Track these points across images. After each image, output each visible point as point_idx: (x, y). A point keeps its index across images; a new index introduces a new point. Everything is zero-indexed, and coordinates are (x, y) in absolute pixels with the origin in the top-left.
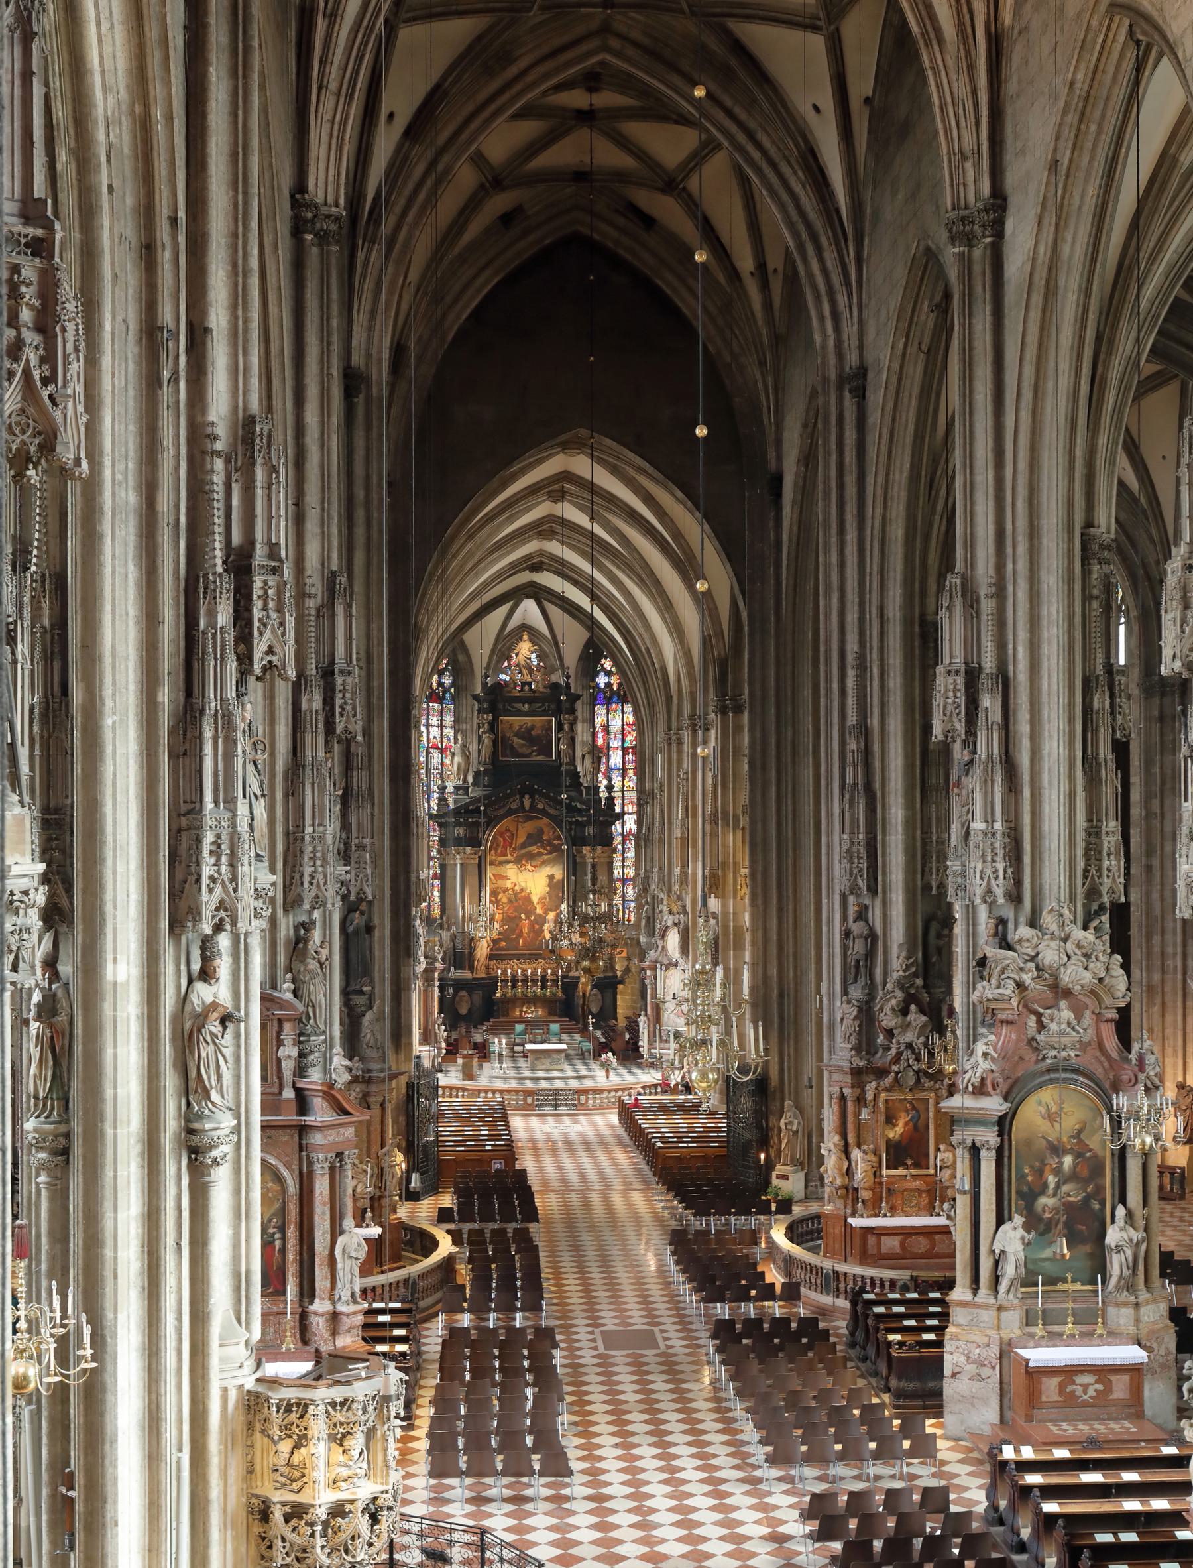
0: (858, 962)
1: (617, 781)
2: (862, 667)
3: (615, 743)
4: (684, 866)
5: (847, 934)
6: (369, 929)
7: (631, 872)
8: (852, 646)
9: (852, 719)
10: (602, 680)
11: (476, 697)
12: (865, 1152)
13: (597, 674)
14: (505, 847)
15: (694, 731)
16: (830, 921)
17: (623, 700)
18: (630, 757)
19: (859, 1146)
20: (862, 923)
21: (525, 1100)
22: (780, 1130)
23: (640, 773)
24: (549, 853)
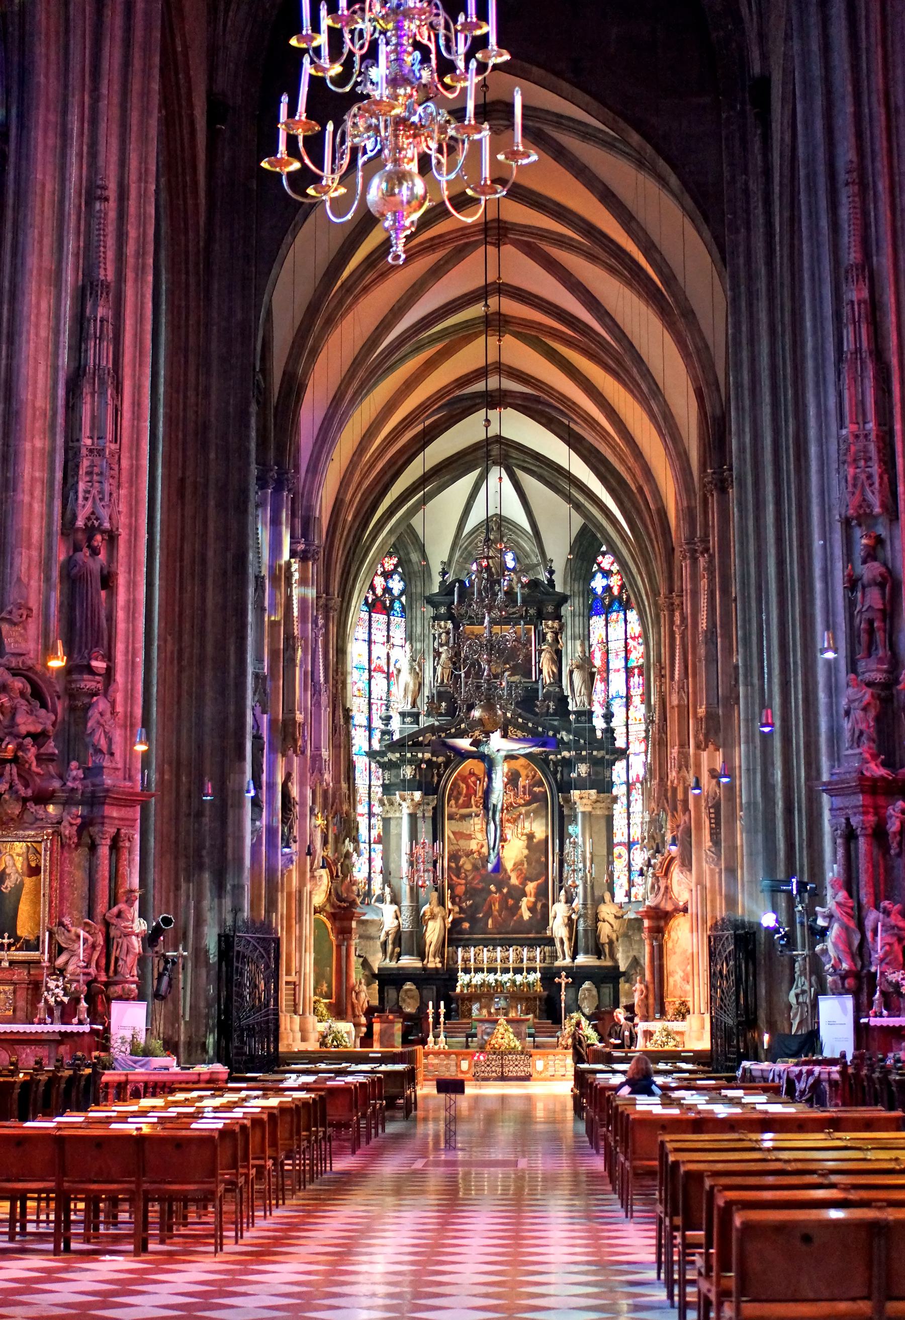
0: (871, 622)
1: (618, 708)
2: (864, 186)
3: (616, 663)
4: (684, 745)
5: (852, 583)
6: (108, 580)
7: (636, 833)
8: (846, 153)
9: (851, 255)
10: (598, 583)
11: (430, 601)
12: (887, 912)
13: (593, 576)
14: (468, 797)
15: (695, 561)
16: (827, 575)
17: (626, 606)
18: (636, 680)
19: (877, 907)
20: (876, 564)
21: (458, 1066)
22: (791, 1007)
23: (646, 698)
24: (528, 803)
